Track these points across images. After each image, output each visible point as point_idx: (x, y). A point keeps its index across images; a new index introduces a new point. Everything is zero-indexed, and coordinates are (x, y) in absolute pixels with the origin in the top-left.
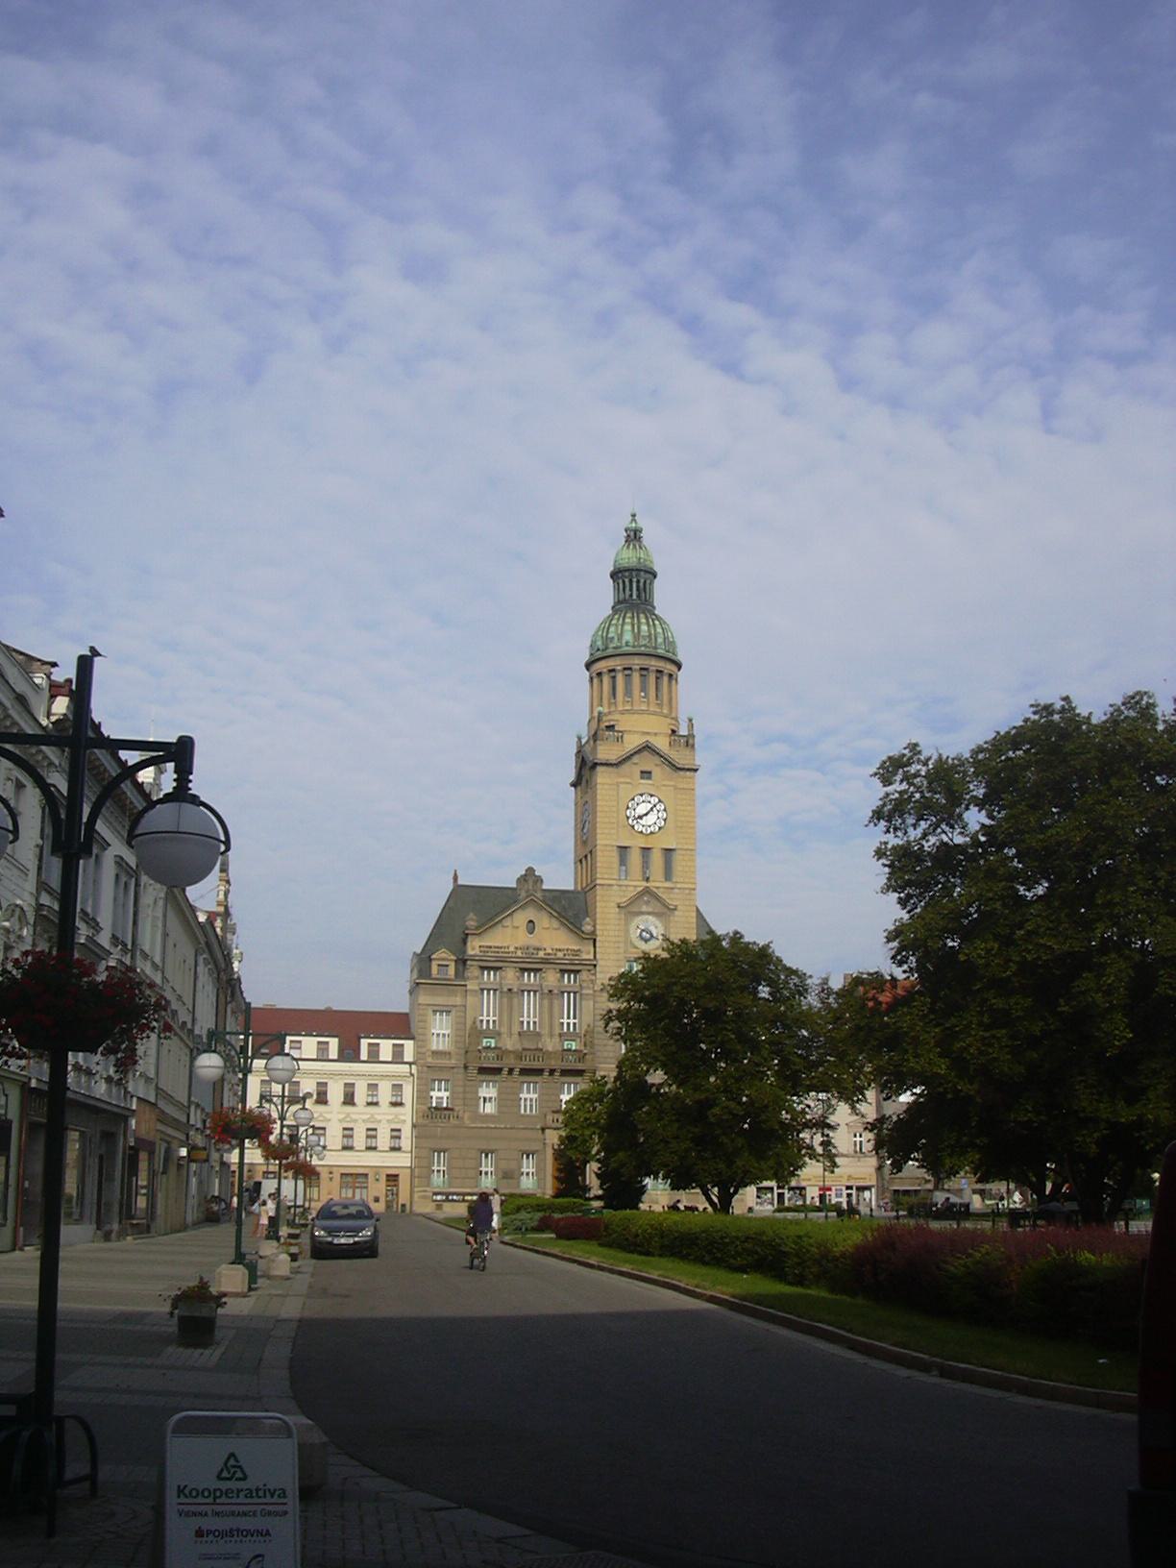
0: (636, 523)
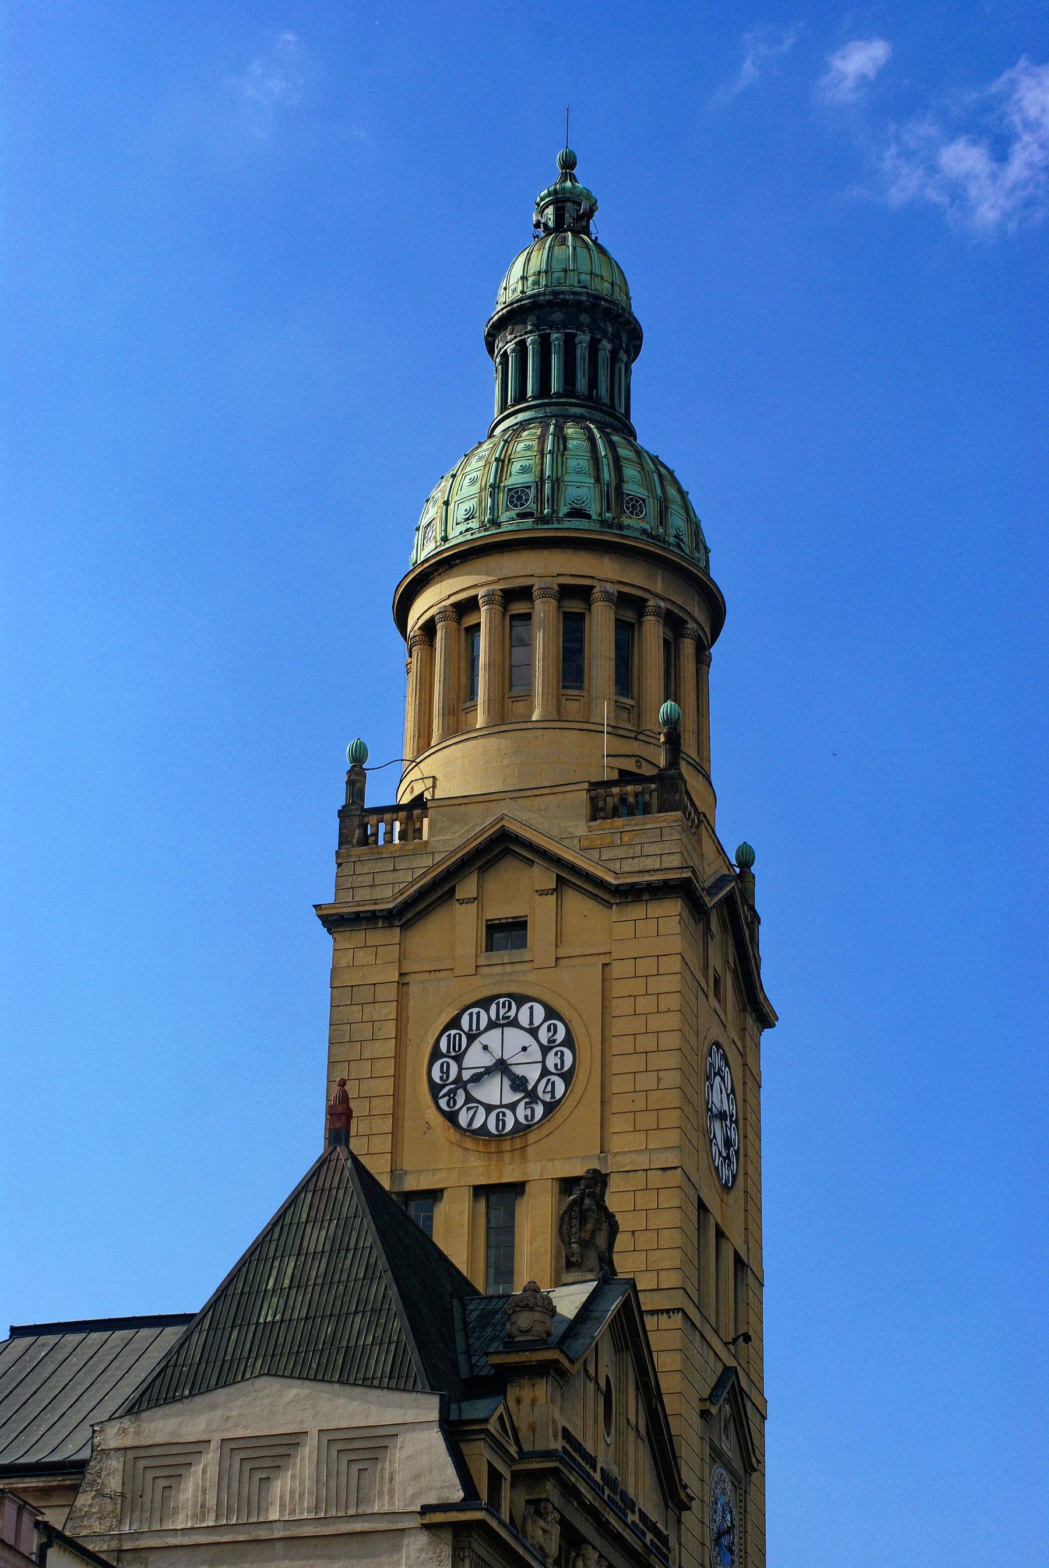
0: (573, 179)
